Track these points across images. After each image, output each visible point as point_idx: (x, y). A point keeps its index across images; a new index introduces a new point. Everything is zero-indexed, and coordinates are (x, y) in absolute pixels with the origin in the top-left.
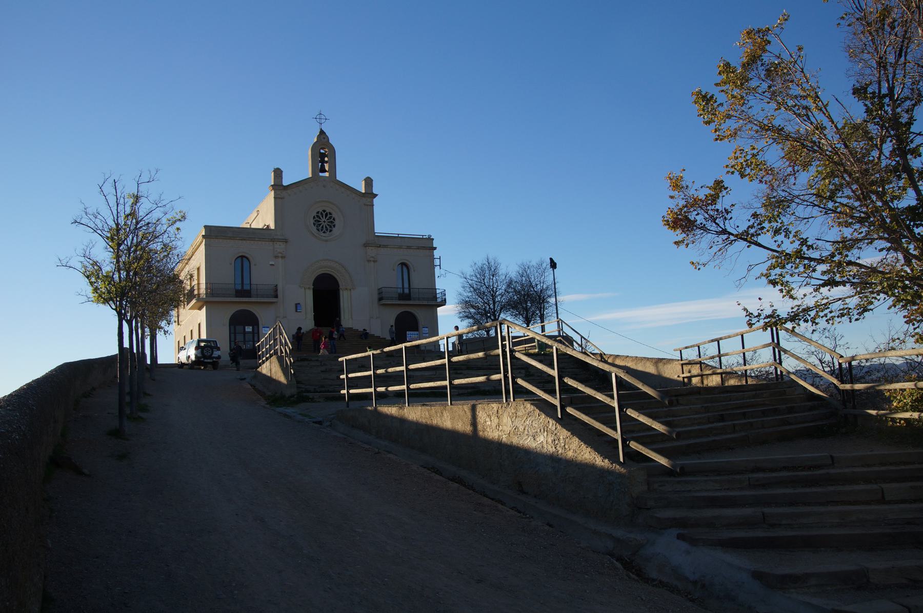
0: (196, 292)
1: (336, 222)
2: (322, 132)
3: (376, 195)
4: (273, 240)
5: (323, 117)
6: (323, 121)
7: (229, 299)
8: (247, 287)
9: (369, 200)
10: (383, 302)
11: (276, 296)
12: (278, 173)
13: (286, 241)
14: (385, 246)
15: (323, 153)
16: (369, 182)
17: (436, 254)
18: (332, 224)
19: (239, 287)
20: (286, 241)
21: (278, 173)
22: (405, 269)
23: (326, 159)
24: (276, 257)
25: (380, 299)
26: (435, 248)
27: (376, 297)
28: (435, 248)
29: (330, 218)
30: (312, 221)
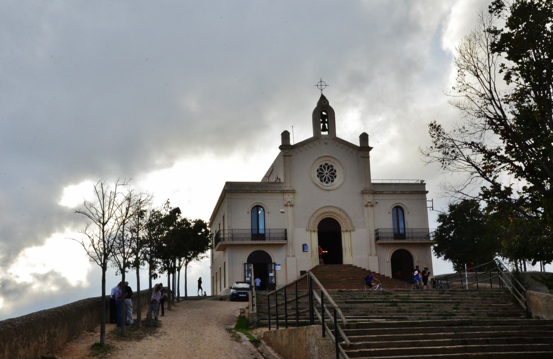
0: (222, 236)
1: (337, 174)
2: (323, 98)
3: (371, 148)
4: (283, 192)
5: (323, 84)
6: (323, 87)
7: (246, 242)
8: (261, 231)
9: (365, 153)
10: (379, 242)
11: (286, 239)
12: (285, 135)
13: (293, 192)
14: (381, 193)
15: (324, 115)
16: (364, 137)
17: (428, 196)
18: (333, 176)
19: (255, 232)
20: (293, 192)
21: (285, 135)
22: (400, 212)
23: (326, 120)
24: (286, 205)
25: (377, 239)
26: (427, 192)
27: (373, 238)
28: (427, 192)
29: (332, 170)
30: (316, 174)
